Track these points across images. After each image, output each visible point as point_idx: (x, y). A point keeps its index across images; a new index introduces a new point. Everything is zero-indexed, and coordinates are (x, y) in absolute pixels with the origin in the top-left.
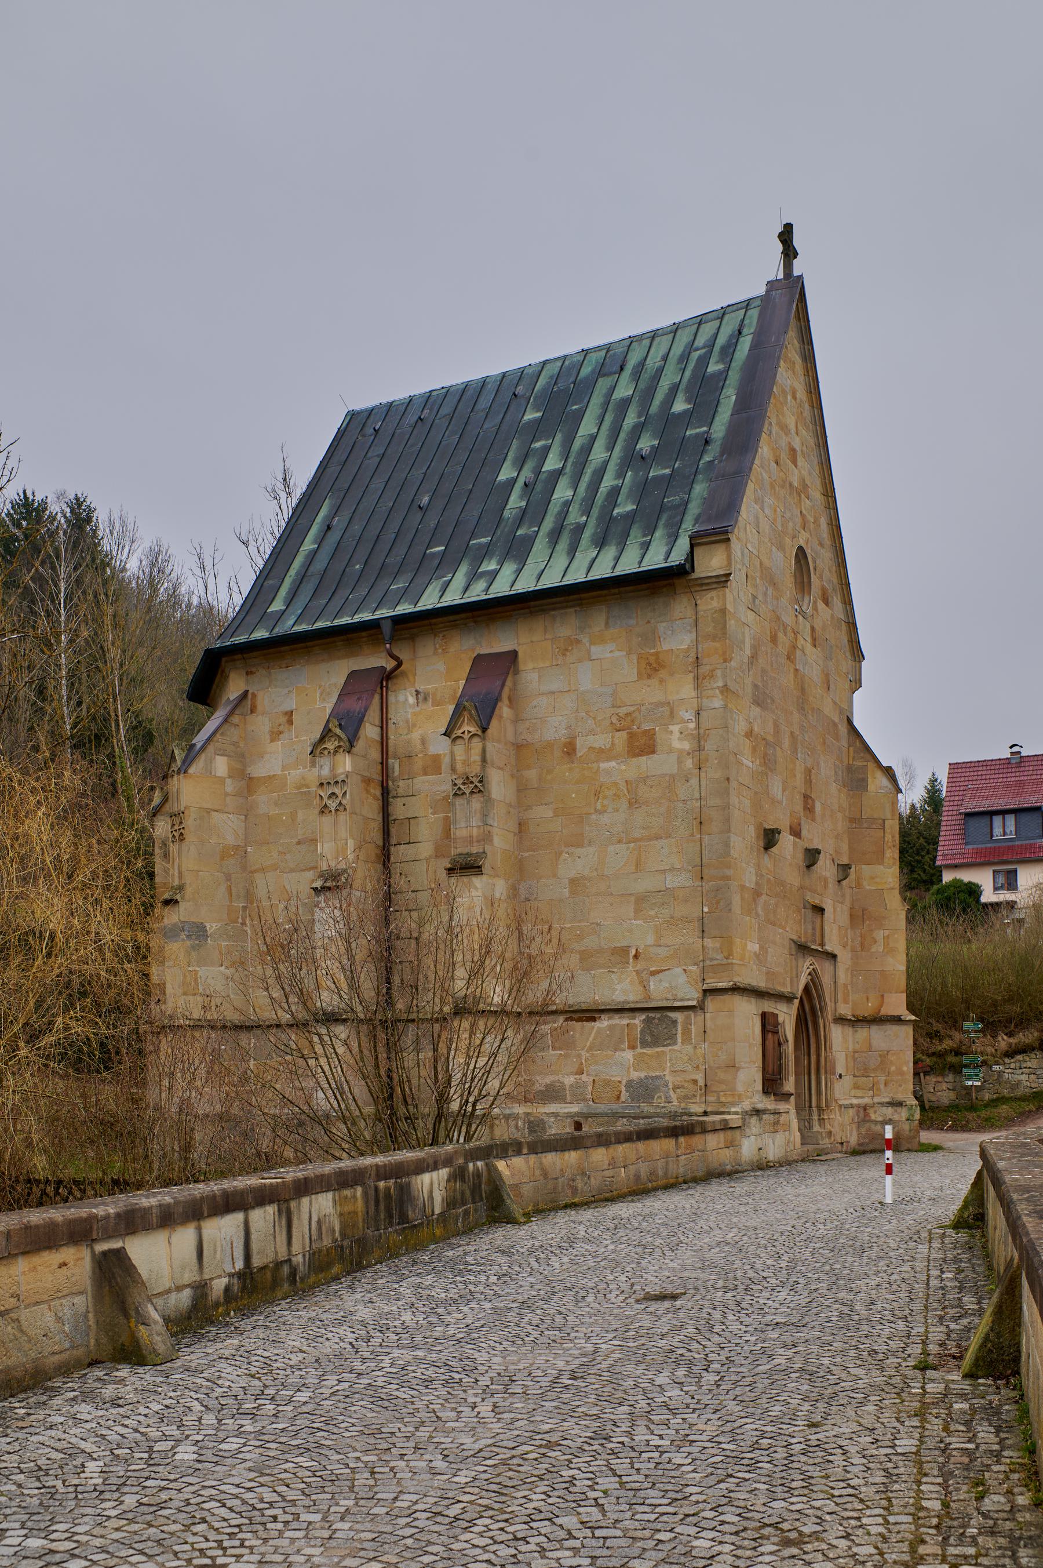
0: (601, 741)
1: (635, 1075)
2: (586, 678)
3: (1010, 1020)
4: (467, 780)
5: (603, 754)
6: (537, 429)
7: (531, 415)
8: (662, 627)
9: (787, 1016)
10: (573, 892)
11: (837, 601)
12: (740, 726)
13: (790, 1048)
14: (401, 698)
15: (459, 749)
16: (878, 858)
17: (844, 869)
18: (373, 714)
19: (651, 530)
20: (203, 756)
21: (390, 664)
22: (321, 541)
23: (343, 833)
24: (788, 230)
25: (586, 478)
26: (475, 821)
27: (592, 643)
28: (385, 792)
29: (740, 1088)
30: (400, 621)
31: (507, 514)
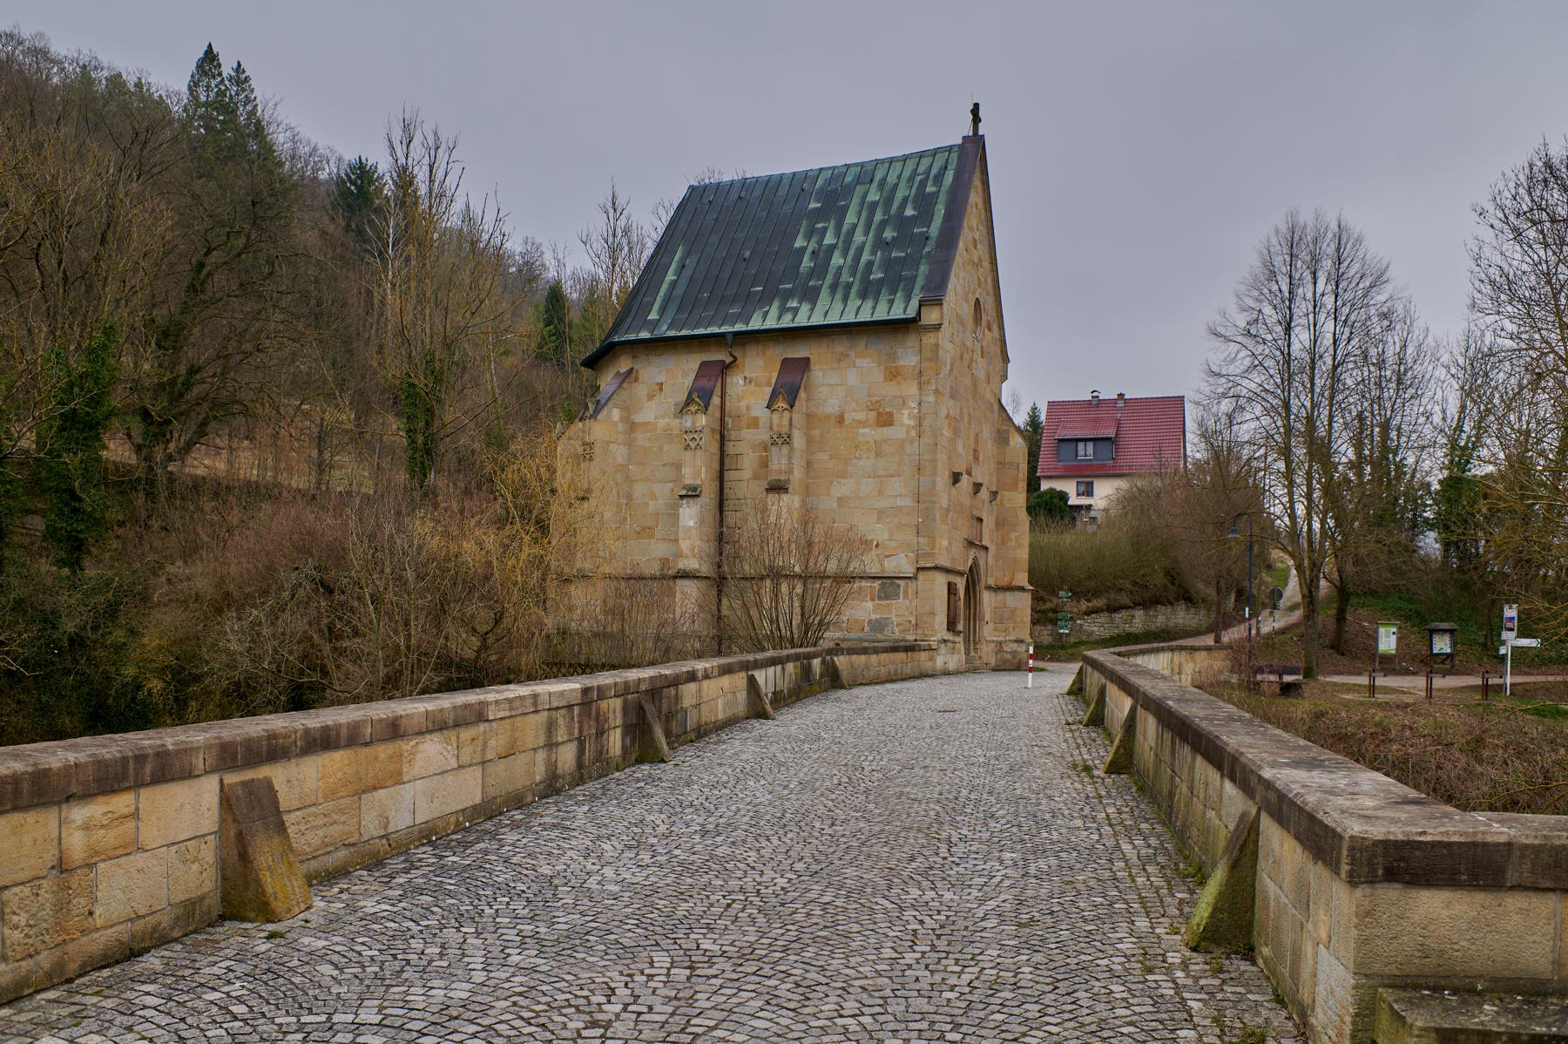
0: (860, 416)
1: (874, 617)
2: (852, 378)
4: (780, 436)
5: (862, 424)
6: (817, 215)
7: (813, 205)
9: (961, 583)
10: (840, 505)
11: (995, 328)
12: (943, 412)
13: (961, 604)
14: (735, 380)
15: (775, 416)
16: (1014, 487)
17: (994, 494)
18: (718, 390)
20: (606, 409)
21: (728, 360)
22: (679, 273)
23: (699, 463)
24: (976, 106)
25: (852, 252)
27: (856, 357)
28: (722, 437)
29: (936, 627)
30: (738, 335)
31: (801, 270)
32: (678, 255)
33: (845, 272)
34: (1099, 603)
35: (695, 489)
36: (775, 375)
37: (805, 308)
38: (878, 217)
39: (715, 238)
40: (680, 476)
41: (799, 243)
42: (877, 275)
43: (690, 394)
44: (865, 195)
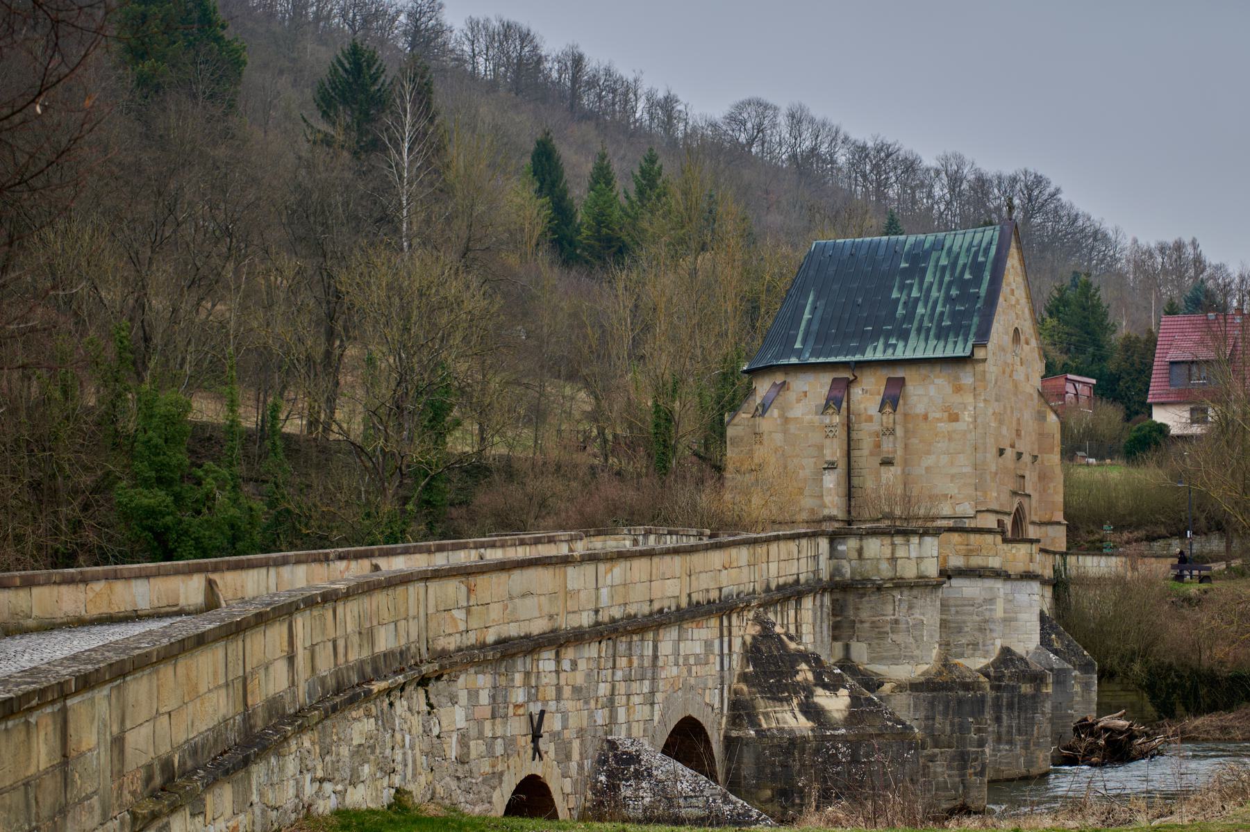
0: (938, 415)
2: (932, 391)
3: (1130, 525)
4: (888, 429)
6: (907, 273)
7: (903, 265)
8: (961, 375)
10: (927, 472)
12: (991, 411)
14: (856, 390)
15: (884, 417)
16: (1051, 450)
17: (1035, 457)
19: (957, 336)
21: (852, 378)
25: (930, 304)
31: (897, 315)
33: (926, 319)
34: (1140, 533)
35: (833, 464)
37: (901, 345)
38: (947, 278)
39: (836, 287)
40: (823, 456)
42: (946, 323)
43: (828, 401)
44: (938, 259)
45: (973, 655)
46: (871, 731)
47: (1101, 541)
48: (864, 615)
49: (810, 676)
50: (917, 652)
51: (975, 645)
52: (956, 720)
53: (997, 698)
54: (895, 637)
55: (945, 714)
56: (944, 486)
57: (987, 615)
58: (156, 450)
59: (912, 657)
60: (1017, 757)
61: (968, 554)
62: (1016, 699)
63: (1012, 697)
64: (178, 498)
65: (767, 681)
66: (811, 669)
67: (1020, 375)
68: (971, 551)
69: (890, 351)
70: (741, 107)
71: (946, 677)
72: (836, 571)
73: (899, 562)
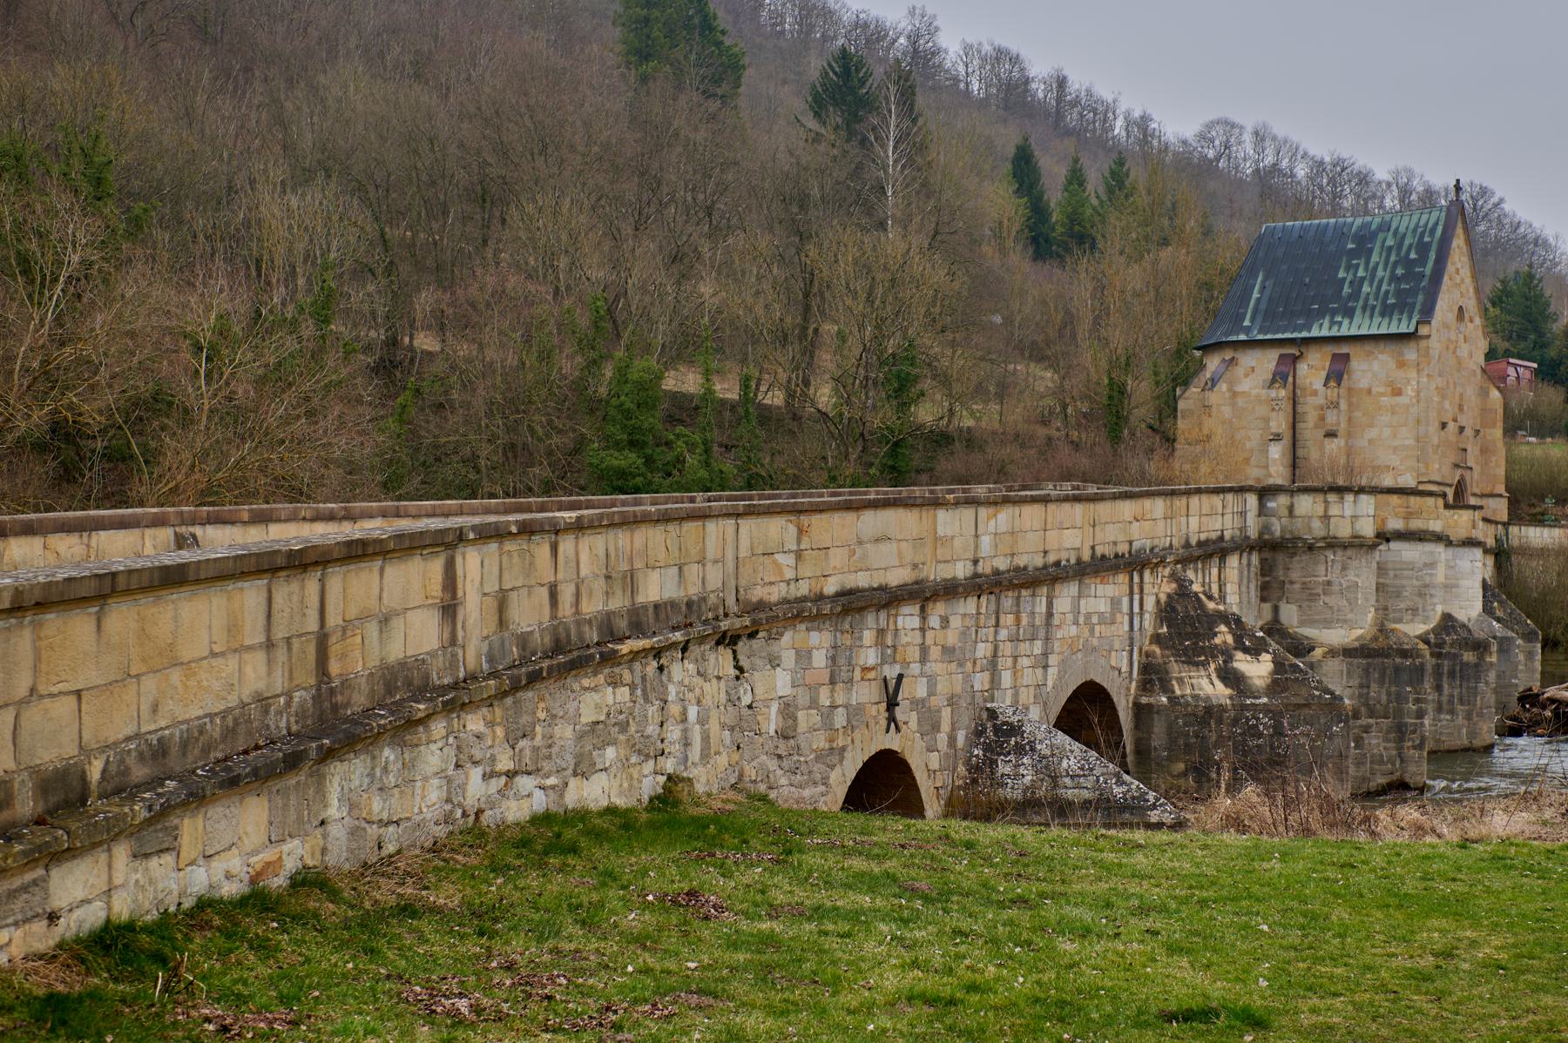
0: (1382, 390)
2: (1376, 366)
5: (1383, 394)
6: (1353, 254)
7: (1350, 246)
8: (1406, 351)
12: (1433, 386)
15: (1329, 391)
16: (1494, 425)
17: (1477, 432)
19: (1401, 313)
21: (1298, 354)
25: (1375, 283)
26: (1335, 418)
28: (1294, 402)
32: (1260, 279)
33: (1371, 297)
36: (1328, 364)
38: (1393, 258)
39: (1284, 267)
40: (1269, 428)
41: (1341, 274)
42: (1391, 301)
43: (1274, 375)
45: (1412, 621)
46: (1294, 700)
47: (1543, 514)
48: (1295, 575)
49: (1230, 639)
50: (1350, 616)
51: (1414, 611)
52: (1393, 689)
53: (1438, 666)
54: (1327, 599)
55: (1381, 682)
56: (1386, 458)
57: (1427, 580)
58: (628, 414)
59: (1345, 621)
60: (1460, 728)
61: (1408, 516)
62: (1458, 668)
63: (1454, 665)
64: (649, 461)
65: (1181, 644)
66: (1231, 631)
67: (1464, 351)
68: (1411, 513)
69: (1335, 328)
70: (1210, 126)
71: (1382, 643)
72: (1265, 529)
73: (1332, 520)
